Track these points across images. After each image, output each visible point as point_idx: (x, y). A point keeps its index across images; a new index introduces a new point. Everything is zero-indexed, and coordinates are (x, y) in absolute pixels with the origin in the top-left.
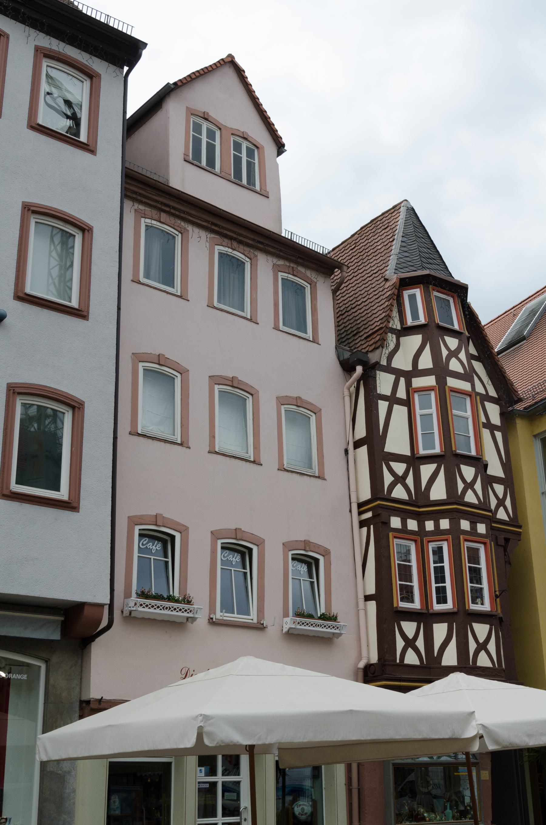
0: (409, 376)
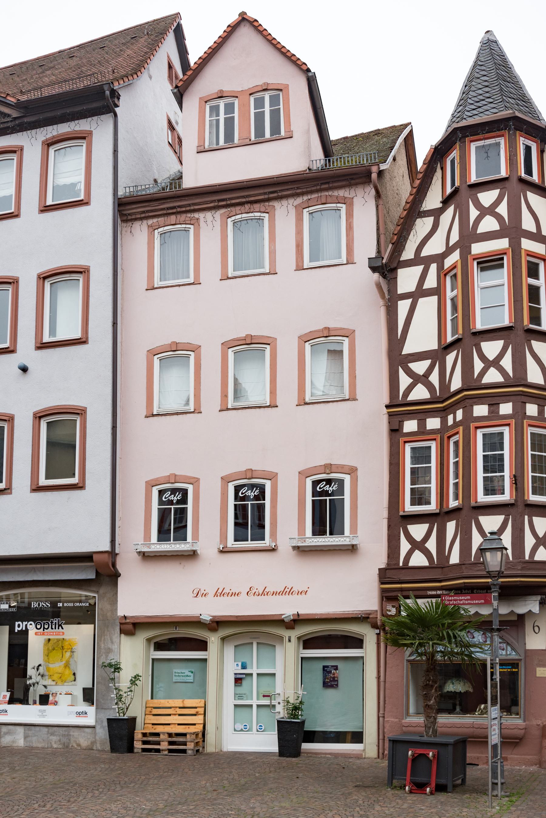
0: (440, 259)
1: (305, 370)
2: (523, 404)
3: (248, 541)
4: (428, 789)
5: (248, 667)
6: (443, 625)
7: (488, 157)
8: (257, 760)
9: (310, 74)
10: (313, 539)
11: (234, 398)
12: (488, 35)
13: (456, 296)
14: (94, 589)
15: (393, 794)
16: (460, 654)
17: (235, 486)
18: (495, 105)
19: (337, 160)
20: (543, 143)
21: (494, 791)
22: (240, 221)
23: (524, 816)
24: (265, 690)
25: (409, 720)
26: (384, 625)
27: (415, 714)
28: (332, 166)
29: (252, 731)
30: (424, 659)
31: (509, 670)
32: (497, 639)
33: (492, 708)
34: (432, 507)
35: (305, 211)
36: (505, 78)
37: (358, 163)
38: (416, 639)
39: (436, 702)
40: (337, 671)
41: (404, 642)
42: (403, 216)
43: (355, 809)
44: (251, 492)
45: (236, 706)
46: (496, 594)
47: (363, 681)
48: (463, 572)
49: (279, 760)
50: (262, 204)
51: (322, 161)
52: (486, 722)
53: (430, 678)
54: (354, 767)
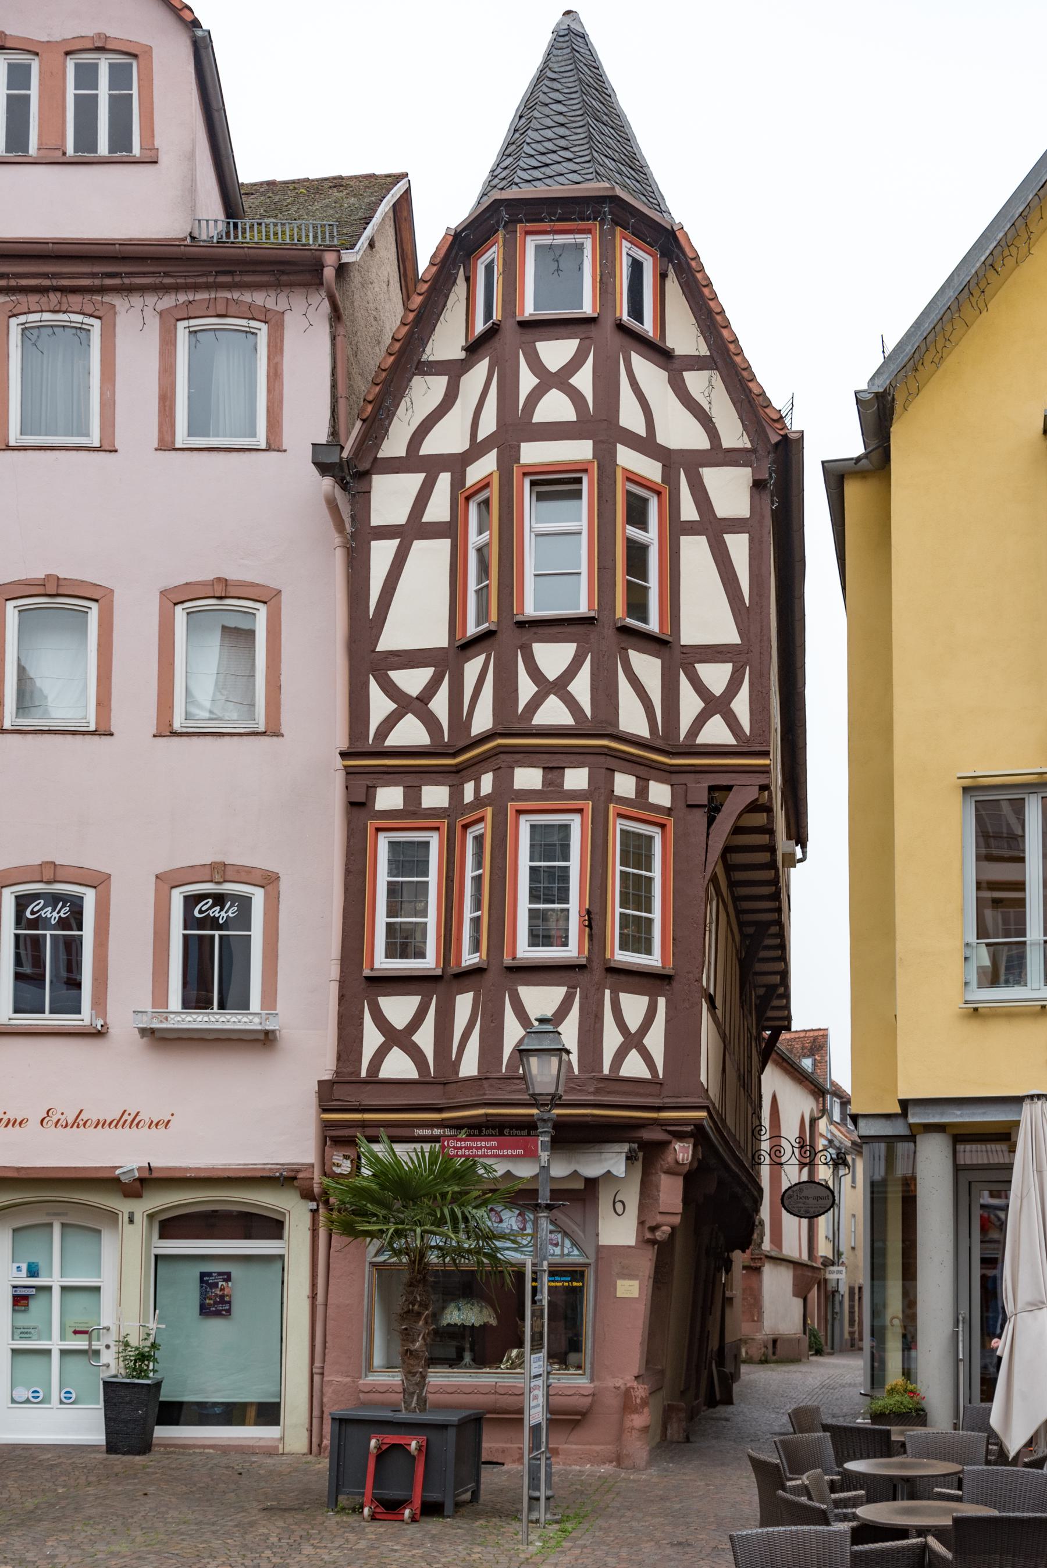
0: (457, 464)
1: (173, 664)
2: (609, 772)
3: (43, 1012)
4: (407, 1512)
5: (41, 1273)
6: (444, 1195)
7: (558, 270)
8: (60, 1460)
9: (199, 33)
10: (183, 1016)
11: (18, 708)
12: (568, 20)
13: (487, 545)
15: (337, 1523)
16: (475, 1252)
17: (17, 897)
18: (577, 167)
19: (252, 227)
20: (666, 259)
21: (533, 1513)
22: (38, 327)
23: (588, 1558)
24: (78, 1320)
25: (372, 1379)
26: (326, 1193)
27: (383, 1367)
28: (240, 239)
29: (49, 1402)
30: (404, 1260)
31: (566, 1284)
32: (545, 1225)
33: (533, 1356)
34: (429, 963)
35: (181, 325)
36: (598, 114)
37: (296, 241)
38: (389, 1222)
39: (426, 1345)
40: (230, 1284)
41: (365, 1228)
42: (387, 367)
43: (263, 1552)
44: (53, 910)
45: (15, 1352)
46: (547, 1139)
47: (282, 1303)
48: (485, 1094)
49: (106, 1459)
50: (88, 297)
51: (220, 224)
52: (520, 1383)
53: (415, 1297)
54: (262, 1472)
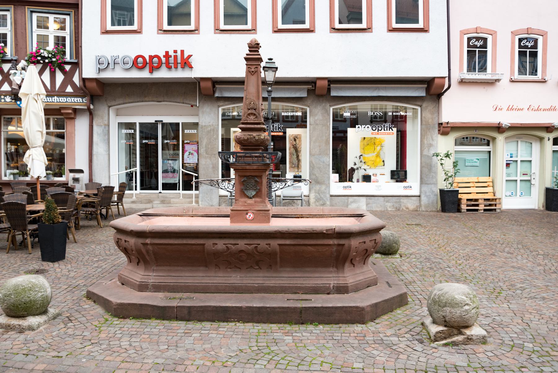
14: (419, 103)
